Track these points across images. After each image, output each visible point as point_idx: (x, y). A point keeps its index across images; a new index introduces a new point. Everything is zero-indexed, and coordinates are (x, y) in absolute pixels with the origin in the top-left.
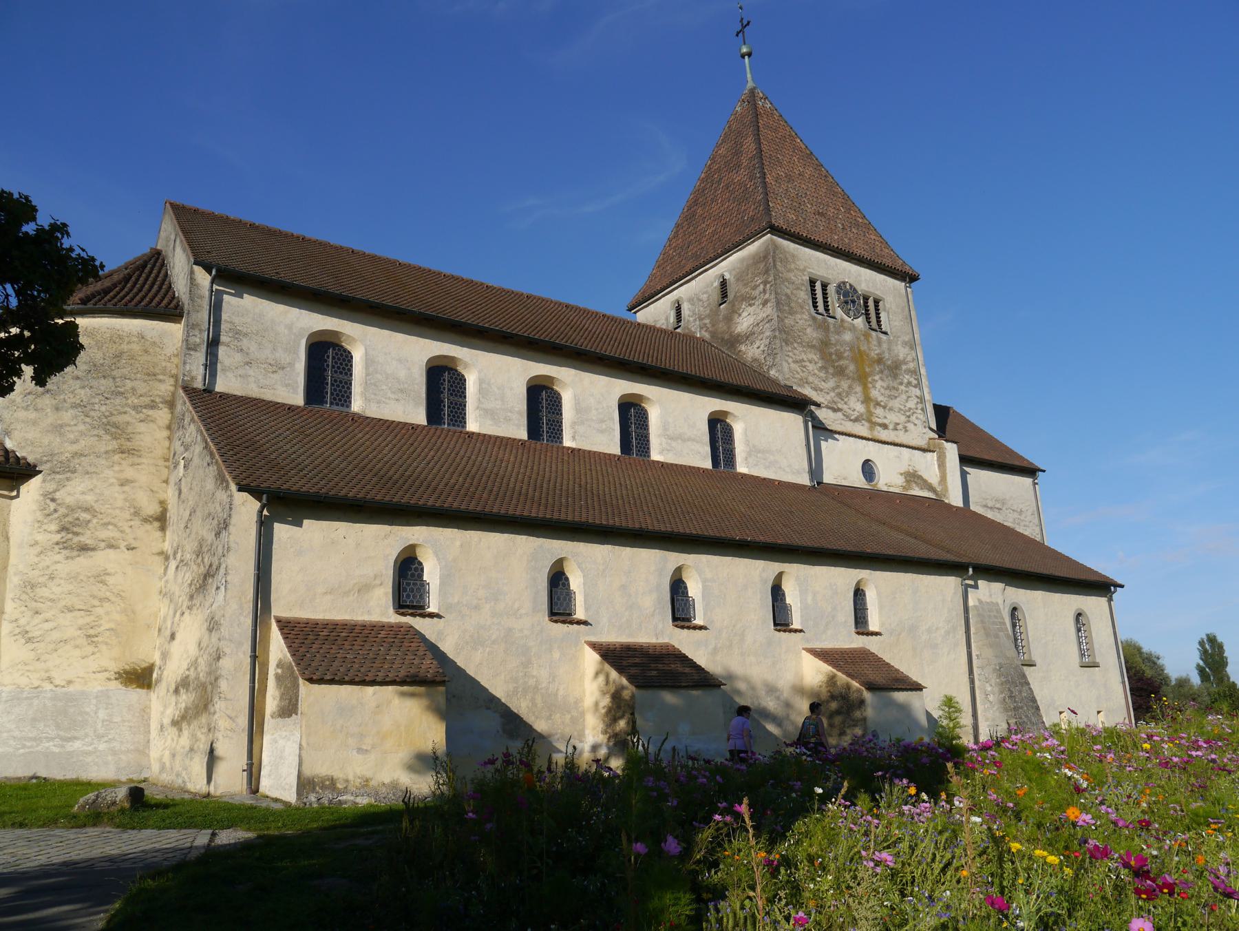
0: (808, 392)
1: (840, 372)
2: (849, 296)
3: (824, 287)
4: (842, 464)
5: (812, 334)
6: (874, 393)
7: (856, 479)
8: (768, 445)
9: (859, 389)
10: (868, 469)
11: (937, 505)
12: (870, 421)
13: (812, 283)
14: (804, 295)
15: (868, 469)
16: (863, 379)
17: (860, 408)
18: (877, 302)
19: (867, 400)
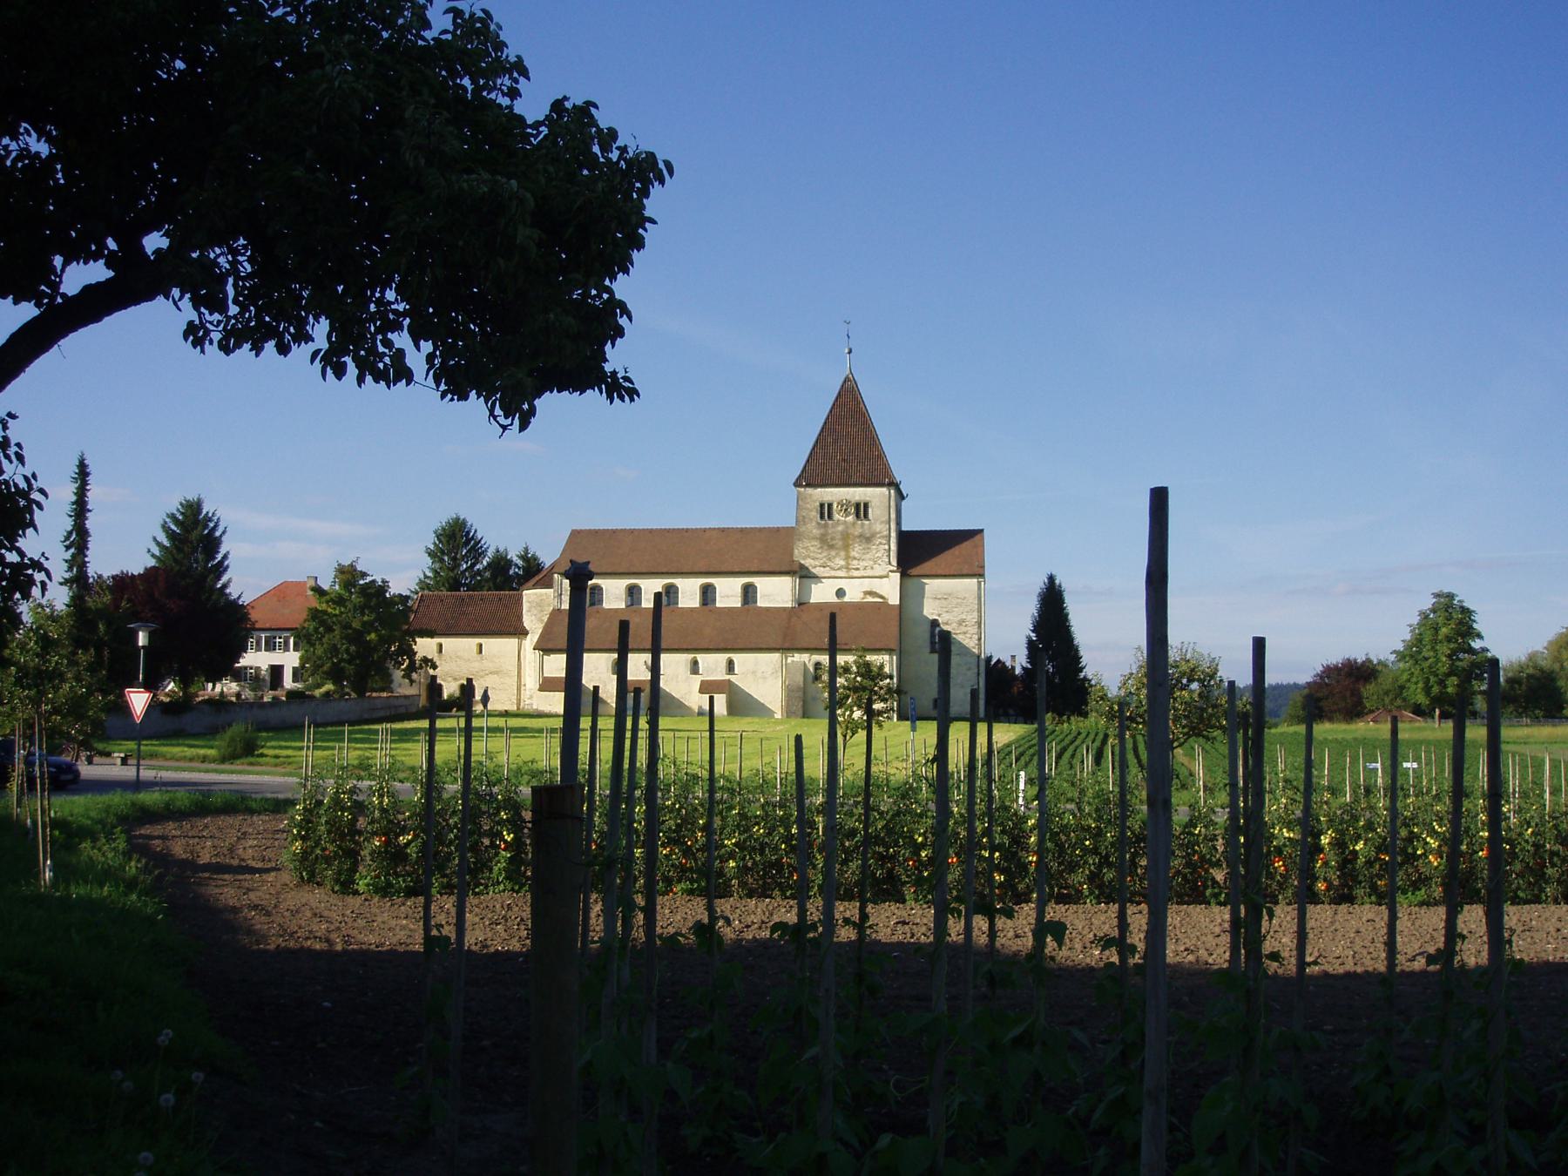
0: (807, 562)
1: (831, 547)
2: (845, 506)
3: (830, 506)
4: (822, 593)
5: (816, 532)
6: (853, 554)
7: (831, 598)
8: (775, 592)
9: (843, 553)
10: (840, 593)
11: (884, 605)
12: (848, 569)
13: (822, 505)
14: (815, 514)
15: (840, 593)
16: (846, 547)
17: (843, 563)
18: (866, 506)
19: (847, 558)
